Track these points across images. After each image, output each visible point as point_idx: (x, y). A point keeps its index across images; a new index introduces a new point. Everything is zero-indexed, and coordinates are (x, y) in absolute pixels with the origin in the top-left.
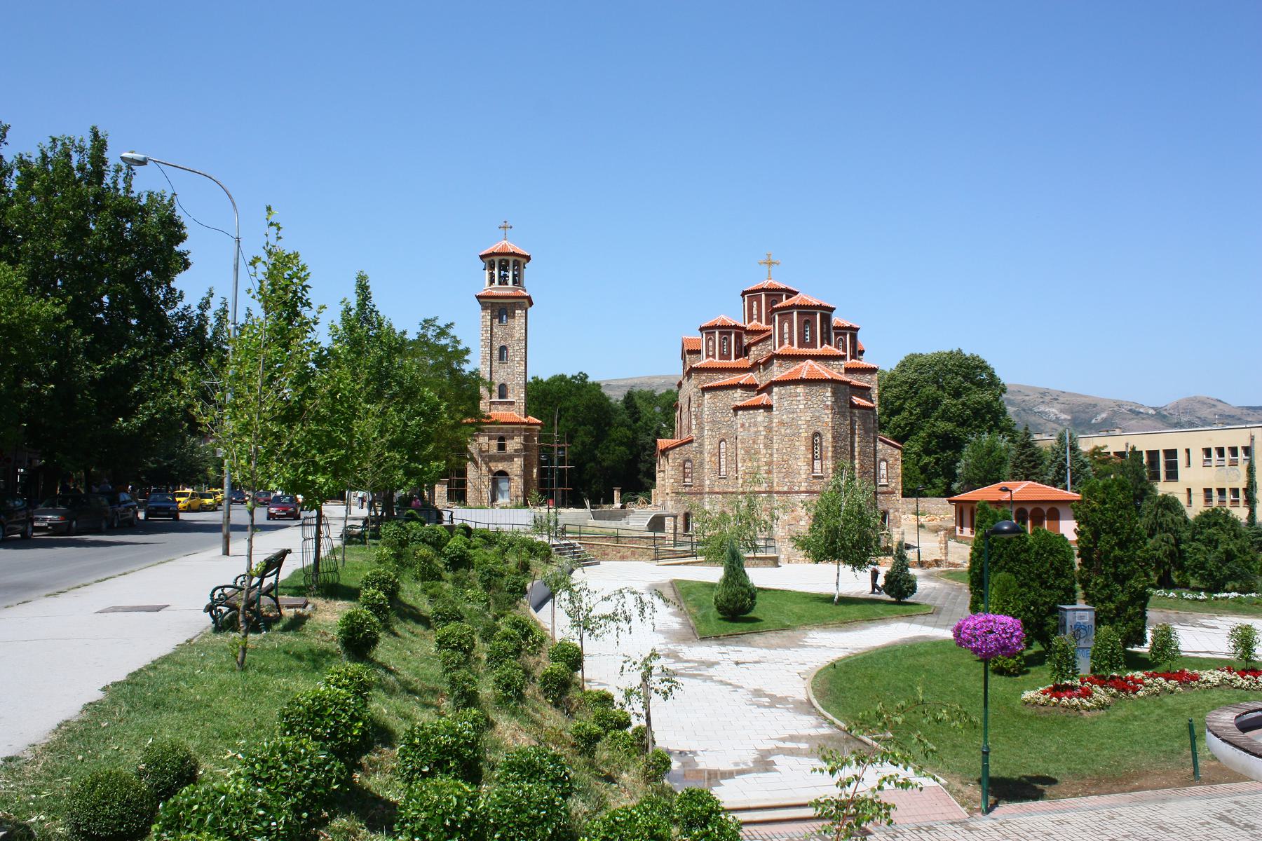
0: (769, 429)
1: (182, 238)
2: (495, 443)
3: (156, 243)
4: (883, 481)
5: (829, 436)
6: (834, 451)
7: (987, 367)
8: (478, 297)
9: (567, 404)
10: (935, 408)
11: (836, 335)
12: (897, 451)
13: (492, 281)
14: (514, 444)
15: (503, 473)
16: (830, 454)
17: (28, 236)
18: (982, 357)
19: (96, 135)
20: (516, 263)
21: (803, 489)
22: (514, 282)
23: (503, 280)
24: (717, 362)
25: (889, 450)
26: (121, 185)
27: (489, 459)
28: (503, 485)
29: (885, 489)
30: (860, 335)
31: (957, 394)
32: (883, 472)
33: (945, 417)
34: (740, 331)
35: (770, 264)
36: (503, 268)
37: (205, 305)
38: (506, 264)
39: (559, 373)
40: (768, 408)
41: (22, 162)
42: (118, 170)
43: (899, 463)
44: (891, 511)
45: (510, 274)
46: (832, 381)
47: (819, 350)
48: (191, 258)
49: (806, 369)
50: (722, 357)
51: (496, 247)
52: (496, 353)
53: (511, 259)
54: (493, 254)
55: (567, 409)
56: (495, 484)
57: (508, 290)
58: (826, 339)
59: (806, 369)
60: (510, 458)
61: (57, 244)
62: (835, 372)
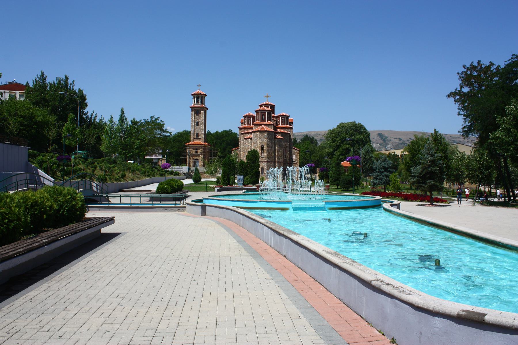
0: (251, 144)
2: (194, 151)
3: (78, 101)
6: (268, 150)
7: (363, 127)
10: (344, 141)
15: (197, 159)
17: (51, 101)
18: (362, 123)
23: (198, 102)
26: (72, 88)
28: (197, 164)
32: (294, 158)
33: (347, 143)
34: (253, 117)
35: (267, 97)
36: (198, 99)
37: (92, 115)
38: (199, 97)
39: (224, 130)
40: (251, 139)
41: (50, 84)
46: (267, 131)
47: (266, 122)
48: (88, 104)
49: (260, 128)
50: (248, 124)
51: (195, 92)
52: (196, 124)
54: (194, 94)
55: (224, 141)
56: (195, 163)
57: (199, 105)
58: (269, 119)
59: (260, 128)
60: (199, 155)
61: (57, 103)
62: (271, 129)
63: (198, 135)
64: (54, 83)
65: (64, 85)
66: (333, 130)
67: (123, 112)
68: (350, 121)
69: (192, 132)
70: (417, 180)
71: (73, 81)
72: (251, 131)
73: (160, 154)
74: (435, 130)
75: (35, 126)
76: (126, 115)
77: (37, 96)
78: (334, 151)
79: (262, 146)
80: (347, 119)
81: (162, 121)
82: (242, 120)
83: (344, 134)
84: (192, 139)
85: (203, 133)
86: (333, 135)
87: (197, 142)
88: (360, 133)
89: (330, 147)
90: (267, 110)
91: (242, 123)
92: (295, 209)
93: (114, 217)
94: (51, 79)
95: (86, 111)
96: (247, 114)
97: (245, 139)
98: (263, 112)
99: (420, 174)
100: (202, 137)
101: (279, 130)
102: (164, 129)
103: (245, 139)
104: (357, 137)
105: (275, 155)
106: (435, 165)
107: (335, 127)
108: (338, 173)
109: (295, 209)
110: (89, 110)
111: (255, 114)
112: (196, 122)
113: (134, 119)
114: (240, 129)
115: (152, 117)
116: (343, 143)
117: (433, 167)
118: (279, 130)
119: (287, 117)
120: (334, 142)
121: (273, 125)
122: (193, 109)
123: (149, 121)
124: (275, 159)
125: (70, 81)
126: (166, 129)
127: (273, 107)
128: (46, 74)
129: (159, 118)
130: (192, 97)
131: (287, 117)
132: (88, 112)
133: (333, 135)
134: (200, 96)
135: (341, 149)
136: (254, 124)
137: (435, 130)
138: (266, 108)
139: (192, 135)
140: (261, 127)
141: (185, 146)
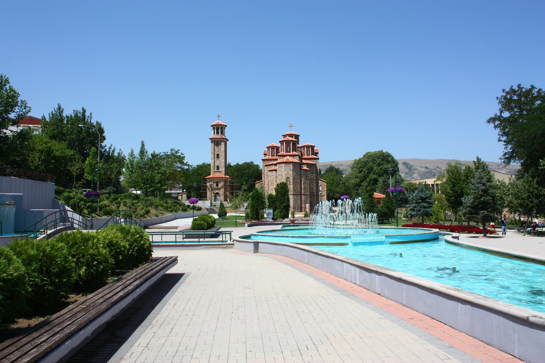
0: (276, 177)
1: (104, 133)
6: (294, 182)
9: (246, 171)
10: (371, 171)
13: (214, 134)
14: (221, 185)
15: (218, 193)
17: (68, 135)
18: (390, 152)
19: (83, 109)
22: (221, 134)
23: (218, 133)
24: (270, 157)
25: (323, 183)
26: (89, 121)
27: (213, 189)
28: (218, 198)
30: (315, 148)
31: (379, 165)
33: (374, 174)
34: (277, 148)
35: (291, 126)
36: (218, 130)
38: (219, 128)
39: (245, 161)
40: (276, 170)
41: (67, 117)
42: (88, 117)
46: (292, 162)
47: (291, 153)
48: (106, 137)
49: (285, 159)
50: (272, 156)
51: (215, 123)
52: (216, 156)
53: (220, 126)
54: (214, 125)
55: (245, 173)
56: (215, 197)
58: (294, 149)
59: (285, 159)
60: (220, 189)
62: (296, 160)
63: (218, 168)
64: (71, 116)
65: (80, 118)
66: (360, 160)
67: (143, 145)
68: (377, 150)
69: (212, 165)
70: (469, 211)
71: (91, 114)
72: (275, 162)
73: (179, 188)
74: (478, 158)
75: (53, 161)
76: (147, 148)
77: (54, 130)
78: (361, 181)
79: (288, 178)
80: (374, 148)
81: (182, 154)
82: (265, 151)
83: (371, 164)
84: (212, 172)
85: (224, 165)
86: (360, 165)
87: (217, 175)
88: (388, 162)
89: (356, 177)
90: (292, 141)
91: (265, 155)
92: (355, 244)
93: (177, 257)
94: (68, 112)
95: (103, 144)
96: (270, 145)
97: (270, 171)
98: (288, 142)
99: (472, 204)
100: (222, 169)
101: (304, 161)
102: (185, 162)
103: (270, 171)
104: (385, 167)
105: (301, 187)
106: (488, 194)
107: (362, 156)
108: (371, 205)
109: (355, 244)
110: (107, 143)
111: (279, 145)
112: (216, 154)
113: (154, 152)
114: (263, 160)
115: (172, 150)
116: (370, 173)
117: (485, 196)
118: (304, 161)
119: (313, 147)
120: (360, 172)
121: (298, 155)
122: (213, 140)
123: (169, 153)
124: (301, 192)
125: (87, 114)
126: (187, 163)
127: (297, 137)
128: (62, 107)
129: (179, 150)
130: (212, 128)
131: (313, 147)
132: (106, 146)
133: (360, 165)
134: (220, 126)
135: (368, 179)
136: (279, 156)
137: (478, 158)
138: (290, 139)
139: (212, 168)
140: (286, 158)
141: (205, 180)
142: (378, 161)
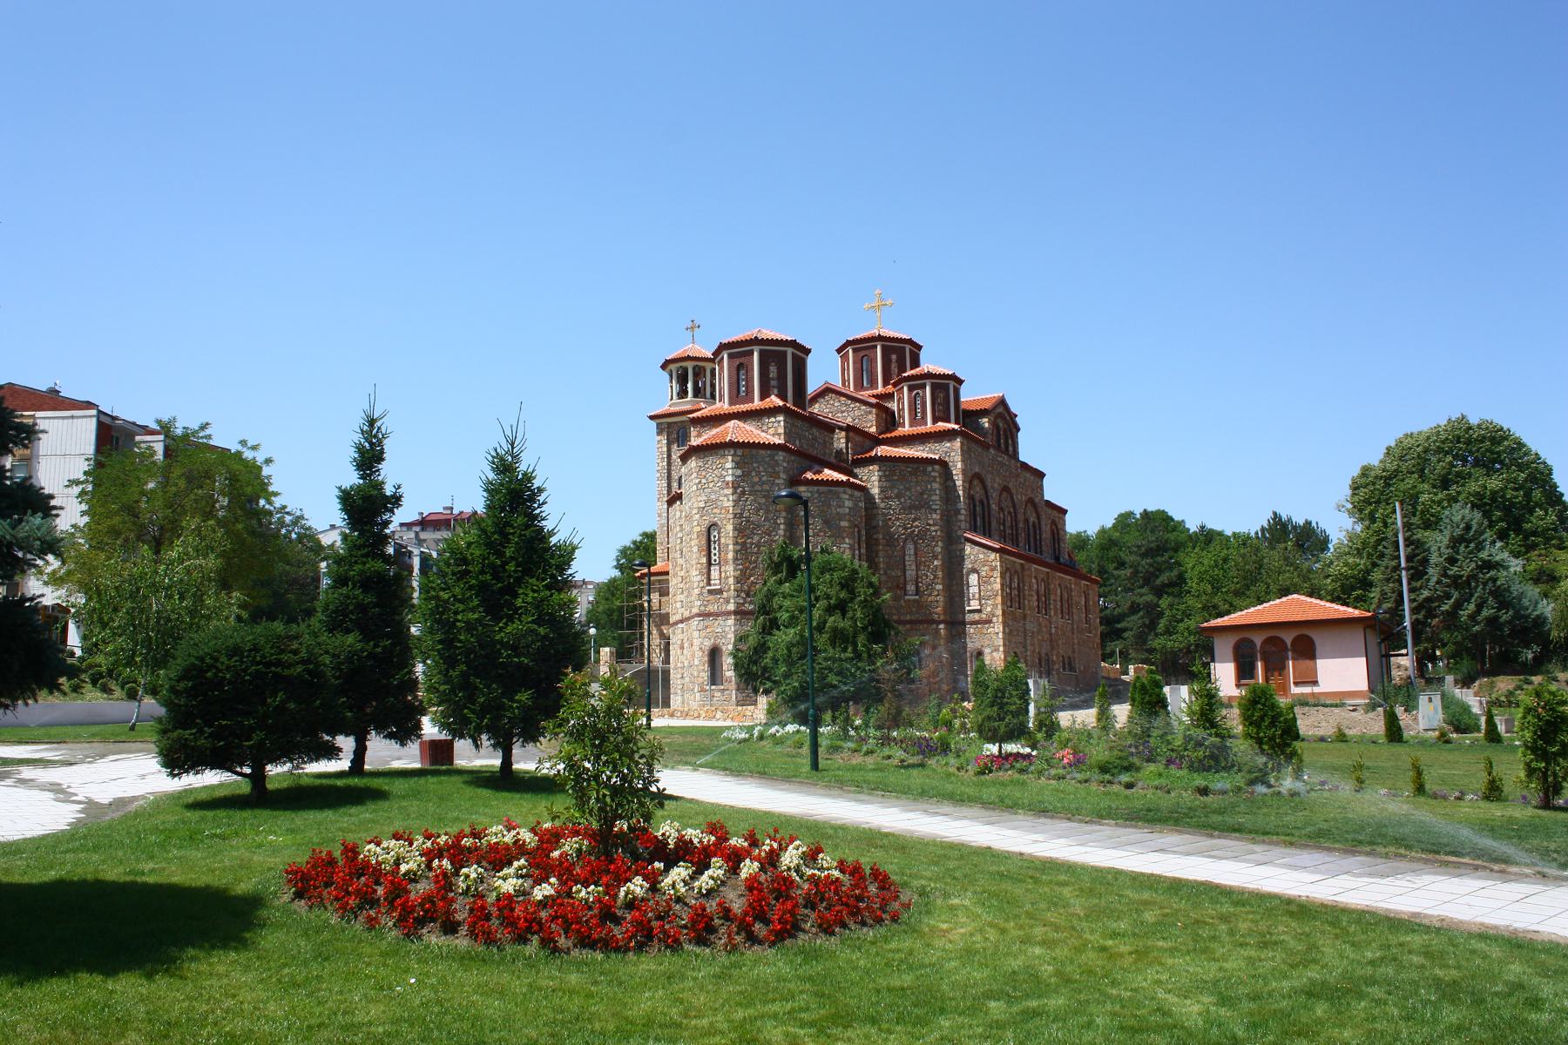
4: (974, 605)
5: (730, 527)
8: (652, 418)
11: (911, 389)
12: (993, 556)
16: (731, 555)
20: (699, 373)
21: (695, 610)
22: (696, 395)
23: (683, 393)
25: (981, 555)
29: (976, 616)
32: (974, 590)
36: (683, 380)
43: (997, 574)
44: (987, 651)
45: (690, 385)
47: (757, 404)
53: (690, 365)
88: (1489, 463)
112: (675, 476)
142: (1439, 466)
